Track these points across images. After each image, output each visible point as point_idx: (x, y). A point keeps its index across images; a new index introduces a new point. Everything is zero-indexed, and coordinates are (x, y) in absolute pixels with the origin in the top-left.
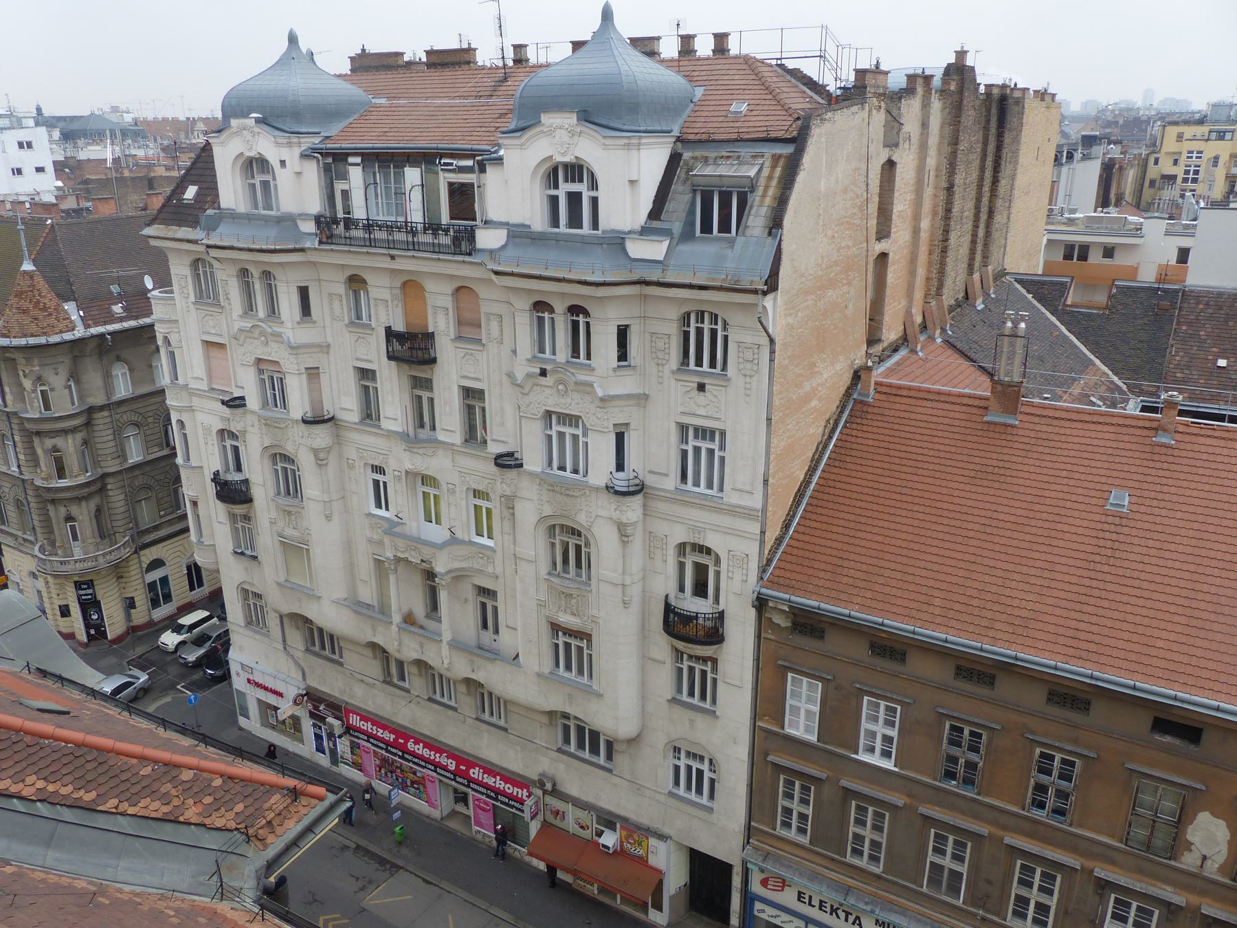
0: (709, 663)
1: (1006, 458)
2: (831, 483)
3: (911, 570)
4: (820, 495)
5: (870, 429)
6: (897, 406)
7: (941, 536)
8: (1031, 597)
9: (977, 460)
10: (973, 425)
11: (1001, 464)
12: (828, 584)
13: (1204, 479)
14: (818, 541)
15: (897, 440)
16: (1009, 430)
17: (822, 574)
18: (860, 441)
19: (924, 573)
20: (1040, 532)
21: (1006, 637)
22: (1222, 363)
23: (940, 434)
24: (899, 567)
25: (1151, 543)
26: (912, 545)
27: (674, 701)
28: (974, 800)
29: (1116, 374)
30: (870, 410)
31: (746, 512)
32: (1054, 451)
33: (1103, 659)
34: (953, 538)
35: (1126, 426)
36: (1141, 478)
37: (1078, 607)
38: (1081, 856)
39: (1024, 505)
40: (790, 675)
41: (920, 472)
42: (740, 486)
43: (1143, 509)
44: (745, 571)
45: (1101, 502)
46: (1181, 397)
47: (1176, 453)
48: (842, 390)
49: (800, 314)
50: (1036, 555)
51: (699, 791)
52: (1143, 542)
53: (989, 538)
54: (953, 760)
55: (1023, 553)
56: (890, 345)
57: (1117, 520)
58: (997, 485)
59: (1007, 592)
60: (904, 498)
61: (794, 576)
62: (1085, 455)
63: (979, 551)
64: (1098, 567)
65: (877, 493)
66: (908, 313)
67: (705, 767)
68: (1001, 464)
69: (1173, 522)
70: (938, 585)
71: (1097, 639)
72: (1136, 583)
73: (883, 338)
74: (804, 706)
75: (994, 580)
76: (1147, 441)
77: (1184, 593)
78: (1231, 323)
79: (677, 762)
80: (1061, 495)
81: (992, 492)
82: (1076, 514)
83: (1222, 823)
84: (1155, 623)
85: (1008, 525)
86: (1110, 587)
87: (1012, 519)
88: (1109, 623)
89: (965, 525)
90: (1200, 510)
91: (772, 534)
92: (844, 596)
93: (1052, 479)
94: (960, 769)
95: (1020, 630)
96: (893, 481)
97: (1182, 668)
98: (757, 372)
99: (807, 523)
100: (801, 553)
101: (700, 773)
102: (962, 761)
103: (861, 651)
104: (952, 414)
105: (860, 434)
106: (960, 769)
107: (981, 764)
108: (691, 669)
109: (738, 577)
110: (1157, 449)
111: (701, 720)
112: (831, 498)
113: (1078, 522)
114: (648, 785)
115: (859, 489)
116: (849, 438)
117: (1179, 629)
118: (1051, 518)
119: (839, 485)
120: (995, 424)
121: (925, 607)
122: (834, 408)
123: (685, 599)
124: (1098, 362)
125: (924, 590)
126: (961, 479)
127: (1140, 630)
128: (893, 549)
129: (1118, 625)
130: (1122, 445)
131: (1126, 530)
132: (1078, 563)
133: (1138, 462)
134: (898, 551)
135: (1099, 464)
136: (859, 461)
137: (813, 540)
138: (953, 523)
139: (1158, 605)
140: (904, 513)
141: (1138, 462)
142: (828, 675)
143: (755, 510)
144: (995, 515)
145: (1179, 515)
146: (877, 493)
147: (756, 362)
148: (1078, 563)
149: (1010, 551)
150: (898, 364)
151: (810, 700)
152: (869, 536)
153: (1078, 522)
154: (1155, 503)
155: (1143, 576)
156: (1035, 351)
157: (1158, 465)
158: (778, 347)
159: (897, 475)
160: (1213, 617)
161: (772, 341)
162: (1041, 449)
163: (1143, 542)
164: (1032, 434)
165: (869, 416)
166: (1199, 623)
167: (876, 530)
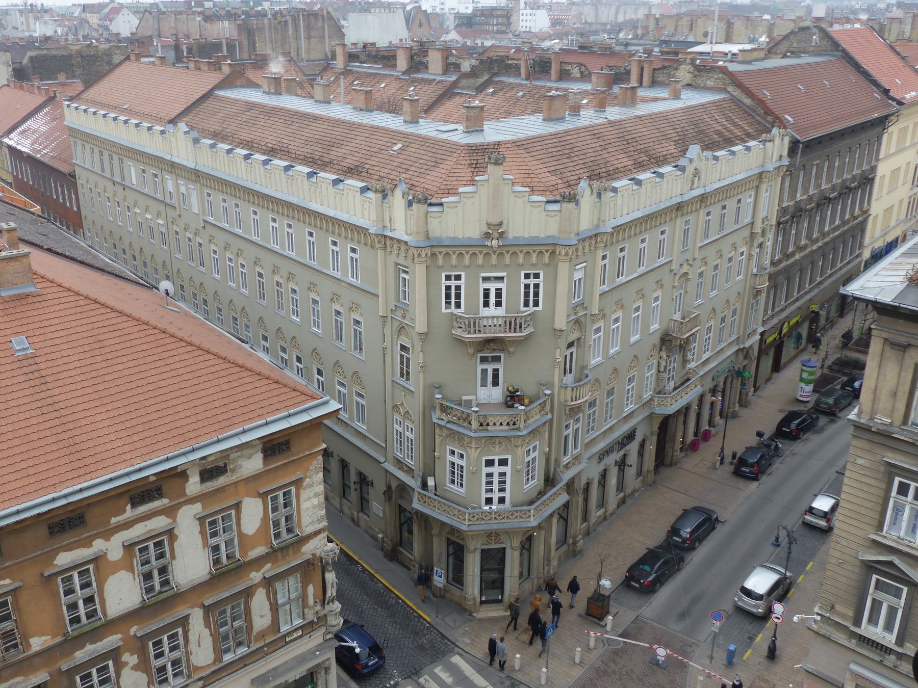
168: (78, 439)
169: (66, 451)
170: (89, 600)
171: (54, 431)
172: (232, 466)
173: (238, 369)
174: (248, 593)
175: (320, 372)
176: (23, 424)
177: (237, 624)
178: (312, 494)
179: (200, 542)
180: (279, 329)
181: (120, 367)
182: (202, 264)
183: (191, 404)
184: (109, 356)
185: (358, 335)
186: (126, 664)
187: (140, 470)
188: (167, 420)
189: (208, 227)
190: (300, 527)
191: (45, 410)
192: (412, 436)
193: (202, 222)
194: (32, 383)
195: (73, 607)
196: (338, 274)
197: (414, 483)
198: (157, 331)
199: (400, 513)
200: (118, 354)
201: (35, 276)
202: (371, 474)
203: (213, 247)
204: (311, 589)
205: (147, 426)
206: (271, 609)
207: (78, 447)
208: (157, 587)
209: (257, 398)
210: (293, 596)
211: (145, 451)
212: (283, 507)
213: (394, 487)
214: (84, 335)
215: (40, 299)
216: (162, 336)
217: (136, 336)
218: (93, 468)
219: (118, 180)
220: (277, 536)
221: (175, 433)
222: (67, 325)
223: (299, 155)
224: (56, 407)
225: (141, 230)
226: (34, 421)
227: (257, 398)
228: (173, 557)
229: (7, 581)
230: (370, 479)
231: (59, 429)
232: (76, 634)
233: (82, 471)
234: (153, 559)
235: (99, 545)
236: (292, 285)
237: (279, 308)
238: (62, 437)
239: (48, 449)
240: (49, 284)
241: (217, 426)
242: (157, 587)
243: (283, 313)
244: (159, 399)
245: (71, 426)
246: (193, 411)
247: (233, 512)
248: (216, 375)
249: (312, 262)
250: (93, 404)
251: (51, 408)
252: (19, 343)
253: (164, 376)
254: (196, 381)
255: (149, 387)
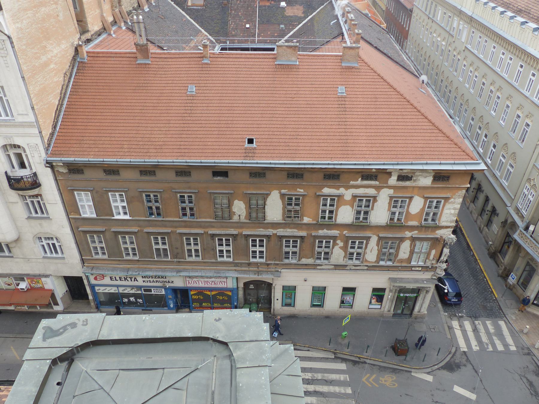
0: (39, 197)
1: (147, 79)
2: (73, 103)
3: (113, 135)
4: (69, 110)
5: (88, 75)
6: (98, 62)
7: (124, 118)
8: (162, 136)
9: (135, 82)
10: (132, 66)
11: (145, 82)
12: (78, 149)
13: (221, 75)
14: (71, 131)
15: (100, 78)
16: (147, 66)
17: (75, 145)
18: (83, 81)
19: (119, 135)
20: (164, 108)
21: (155, 154)
22: (248, 26)
23: (119, 72)
24: (108, 135)
25: (204, 105)
26: (112, 124)
27: (29, 218)
28: (162, 220)
29: (210, 35)
30: (86, 66)
31: (28, 124)
32: (166, 73)
33: (191, 154)
34: (129, 118)
35: (192, 57)
36: (199, 79)
37: (180, 136)
38: (203, 228)
39: (156, 98)
40: (75, 192)
41: (112, 91)
42: (21, 113)
43: (200, 91)
44: (38, 152)
45: (185, 91)
46: (208, 42)
47: (211, 66)
48: (70, 58)
49: (24, 22)
50: (163, 118)
51: (56, 252)
52: (201, 105)
53: (144, 115)
54: (150, 208)
55: (158, 118)
56: (96, 33)
57: (192, 98)
58: (145, 91)
59: (153, 136)
60: (106, 104)
61: (62, 149)
62: (178, 72)
63: (140, 121)
64: (186, 118)
65: (94, 104)
66: (102, 17)
67: (55, 241)
68: (145, 82)
69: (211, 95)
70: (125, 139)
71: (188, 147)
72: (200, 122)
73: (90, 29)
74: (86, 204)
75: (148, 132)
76: (200, 63)
77: (216, 122)
78: (249, 8)
79: (42, 244)
80: (170, 91)
81: (143, 94)
82: (176, 98)
83: (242, 202)
84: (207, 136)
85: (151, 108)
86: (191, 125)
87: (152, 105)
88: (191, 140)
89: (133, 111)
90: (220, 88)
91: (46, 133)
92: (86, 153)
93: (166, 85)
94: (155, 210)
95: (159, 151)
96: (100, 97)
97: (217, 151)
98: (7, 54)
99: (65, 123)
100: (64, 138)
101: (54, 245)
102: (154, 207)
103: (101, 175)
104: (123, 62)
105: (83, 78)
106: (155, 210)
107: (161, 207)
108: (32, 202)
109: (36, 155)
110: (204, 66)
111: (45, 223)
112: (74, 110)
113: (177, 101)
114: (32, 257)
115: (86, 104)
116: (78, 81)
117: (215, 136)
118: (167, 101)
119: (77, 103)
120: (141, 64)
121: (121, 150)
122: (67, 67)
123: (16, 171)
124: (203, 31)
125: (120, 143)
126: (130, 91)
127: (202, 140)
128: (104, 128)
129: (195, 140)
130: (191, 66)
131: (195, 101)
132: (179, 118)
133: (197, 72)
134: (107, 128)
135: (183, 76)
136: (84, 91)
137: (69, 131)
138: (128, 111)
139: (208, 129)
140: (107, 111)
141: (197, 72)
142: (91, 188)
143: (32, 122)
144: (145, 105)
145: (213, 91)
146: (94, 104)
147: (5, 49)
148: (179, 118)
149: (152, 118)
150: (101, 42)
151: (88, 201)
152: (93, 124)
153: (177, 101)
154: (205, 88)
155: (202, 118)
156: (174, 28)
157: (205, 72)
158: (14, 40)
159: (102, 94)
160: (226, 129)
161: (9, 37)
162: (161, 73)
163: (201, 105)
164: (157, 66)
165: (86, 69)
166: (222, 133)
167: (96, 121)
168: (349, 141)
169: (342, 145)
170: (331, 212)
171: (341, 134)
172: (415, 178)
173: (438, 131)
174: (402, 240)
175: (494, 146)
176: (329, 127)
177: (391, 251)
178: (452, 207)
179: (387, 207)
180: (482, 116)
181: (381, 113)
182: (456, 71)
183: (407, 141)
184: (378, 106)
185: (525, 132)
186: (338, 244)
187: (370, 164)
188: (392, 145)
189: (466, 51)
190: (439, 221)
191: (340, 123)
192: (532, 199)
193: (464, 47)
194: (340, 109)
195: (324, 211)
196: (527, 94)
197: (521, 224)
198: (405, 100)
199: (507, 236)
200: (383, 106)
201: (359, 59)
202: (499, 210)
203: (465, 63)
204: (433, 252)
205: (381, 145)
206: (410, 252)
207: (347, 145)
208: (361, 219)
209: (441, 149)
210: (423, 251)
211: (376, 156)
212: (434, 207)
213: (509, 221)
214: (371, 93)
215: (358, 70)
216: (407, 103)
217: (394, 100)
218: (350, 156)
219: (431, 16)
220: (426, 220)
221: (393, 153)
222: (365, 86)
223: (535, 16)
224: (346, 123)
225: (433, 46)
226: (334, 127)
227: (441, 149)
228: (372, 209)
229: (302, 191)
230: (497, 212)
231: (343, 134)
232: (321, 223)
233: (345, 156)
234: (363, 206)
235: (342, 191)
236: (499, 94)
237: (486, 105)
238: (342, 138)
239: (335, 141)
240: (364, 64)
241: (414, 156)
242: (361, 219)
243: (487, 108)
244: (392, 134)
245: (348, 134)
246: (406, 145)
247: (408, 200)
248: (425, 131)
249: (515, 83)
250: (362, 127)
251: (343, 123)
252: (341, 90)
253: (400, 124)
254: (413, 131)
255: (390, 127)
